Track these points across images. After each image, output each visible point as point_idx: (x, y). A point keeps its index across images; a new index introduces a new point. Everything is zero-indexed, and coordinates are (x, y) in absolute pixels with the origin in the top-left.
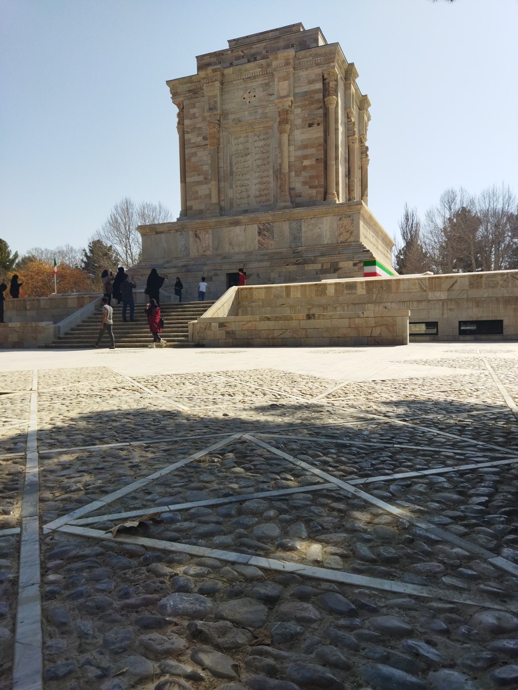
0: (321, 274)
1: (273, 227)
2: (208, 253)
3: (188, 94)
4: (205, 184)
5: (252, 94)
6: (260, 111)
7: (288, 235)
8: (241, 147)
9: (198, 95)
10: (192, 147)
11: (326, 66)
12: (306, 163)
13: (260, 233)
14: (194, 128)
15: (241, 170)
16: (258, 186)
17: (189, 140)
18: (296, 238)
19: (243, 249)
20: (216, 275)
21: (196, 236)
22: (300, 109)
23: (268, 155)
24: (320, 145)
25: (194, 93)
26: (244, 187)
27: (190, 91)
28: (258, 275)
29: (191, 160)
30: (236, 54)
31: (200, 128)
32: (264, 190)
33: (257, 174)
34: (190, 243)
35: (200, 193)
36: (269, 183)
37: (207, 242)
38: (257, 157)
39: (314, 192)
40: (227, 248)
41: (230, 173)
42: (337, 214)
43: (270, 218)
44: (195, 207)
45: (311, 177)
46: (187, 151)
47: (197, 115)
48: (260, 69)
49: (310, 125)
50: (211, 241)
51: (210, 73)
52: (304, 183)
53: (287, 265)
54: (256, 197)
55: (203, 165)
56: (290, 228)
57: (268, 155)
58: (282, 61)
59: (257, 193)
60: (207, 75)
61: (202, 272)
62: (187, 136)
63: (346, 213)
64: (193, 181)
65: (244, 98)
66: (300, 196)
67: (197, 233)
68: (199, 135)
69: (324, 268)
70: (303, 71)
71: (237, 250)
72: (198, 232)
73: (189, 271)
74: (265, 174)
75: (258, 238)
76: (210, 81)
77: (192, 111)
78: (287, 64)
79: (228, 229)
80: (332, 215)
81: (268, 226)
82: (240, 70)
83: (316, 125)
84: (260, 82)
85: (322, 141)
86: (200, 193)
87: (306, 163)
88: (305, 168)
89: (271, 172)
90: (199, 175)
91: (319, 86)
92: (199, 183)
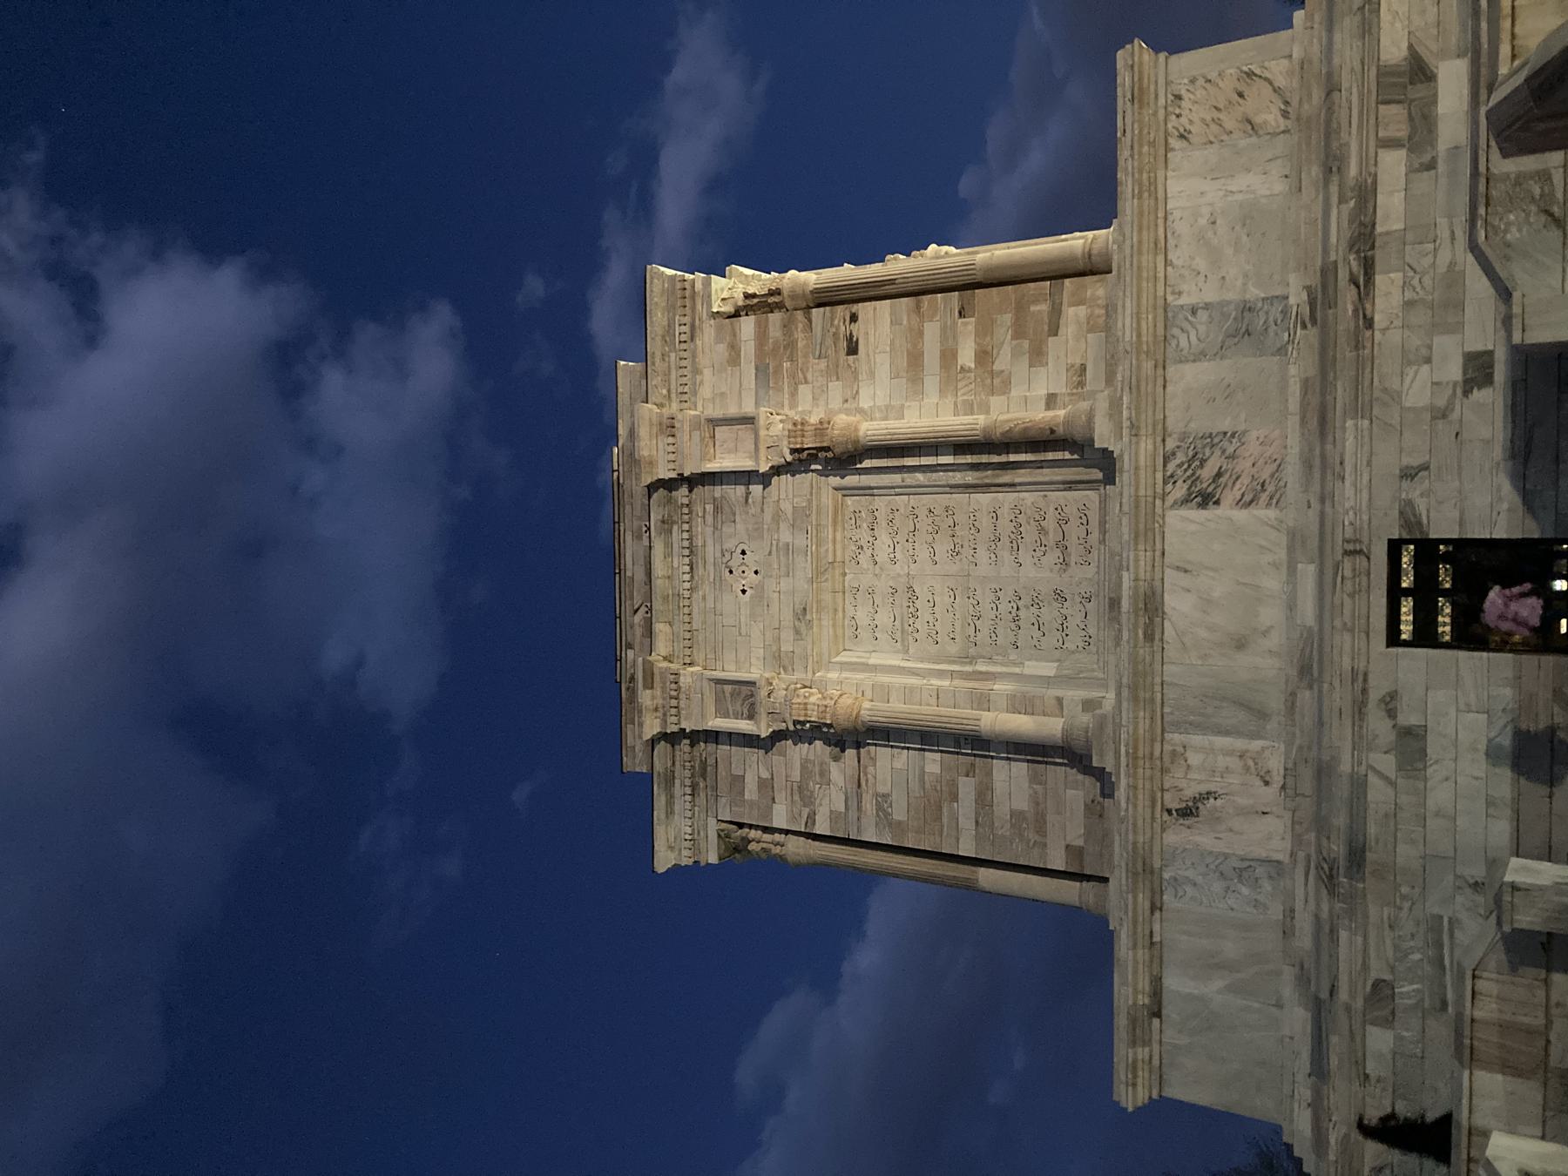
0: (1432, 143)
1: (1183, 437)
2: (1275, 764)
3: (702, 795)
4: (989, 774)
6: (785, 536)
7: (1227, 362)
8: (884, 618)
9: (711, 761)
10: (859, 808)
11: (699, 307)
12: (966, 356)
13: (1206, 500)
14: (803, 794)
15: (958, 624)
16: (1025, 556)
17: (834, 817)
18: (1243, 327)
19: (1273, 583)
20: (1390, 704)
21: (1187, 812)
22: (801, 387)
23: (922, 513)
24: (918, 307)
25: (704, 775)
26: (1022, 613)
27: (694, 787)
28: (1409, 474)
29: (900, 823)
30: (638, 631)
32: (1042, 531)
33: (983, 555)
34: (1220, 847)
35: (1022, 803)
36: (1018, 510)
37: (1222, 761)
38: (923, 553)
39: (1074, 315)
40: (1266, 665)
41: (963, 663)
42: (1162, 151)
43: (1146, 445)
44: (1076, 836)
45: (1018, 334)
47: (765, 775)
48: (675, 527)
49: (853, 349)
50: (1221, 741)
51: (653, 698)
52: (1037, 355)
53: (1369, 323)
54: (1065, 563)
55: (923, 772)
56: (1200, 356)
57: (922, 513)
58: (661, 446)
59: (1054, 556)
60: (656, 710)
61: (1373, 779)
62: (822, 828)
63: (1161, 112)
65: (744, 592)
66: (1083, 368)
67: (1174, 805)
68: (824, 773)
69: (1401, 130)
70: (702, 382)
71: (1270, 615)
73: (1357, 856)
74: (985, 522)
75: (1226, 511)
76: (674, 702)
77: (751, 792)
79: (1171, 652)
80: (1160, 174)
81: (1180, 457)
82: (666, 598)
84: (709, 530)
85: (904, 301)
86: (1022, 803)
89: (984, 499)
91: (747, 325)
92: (984, 797)
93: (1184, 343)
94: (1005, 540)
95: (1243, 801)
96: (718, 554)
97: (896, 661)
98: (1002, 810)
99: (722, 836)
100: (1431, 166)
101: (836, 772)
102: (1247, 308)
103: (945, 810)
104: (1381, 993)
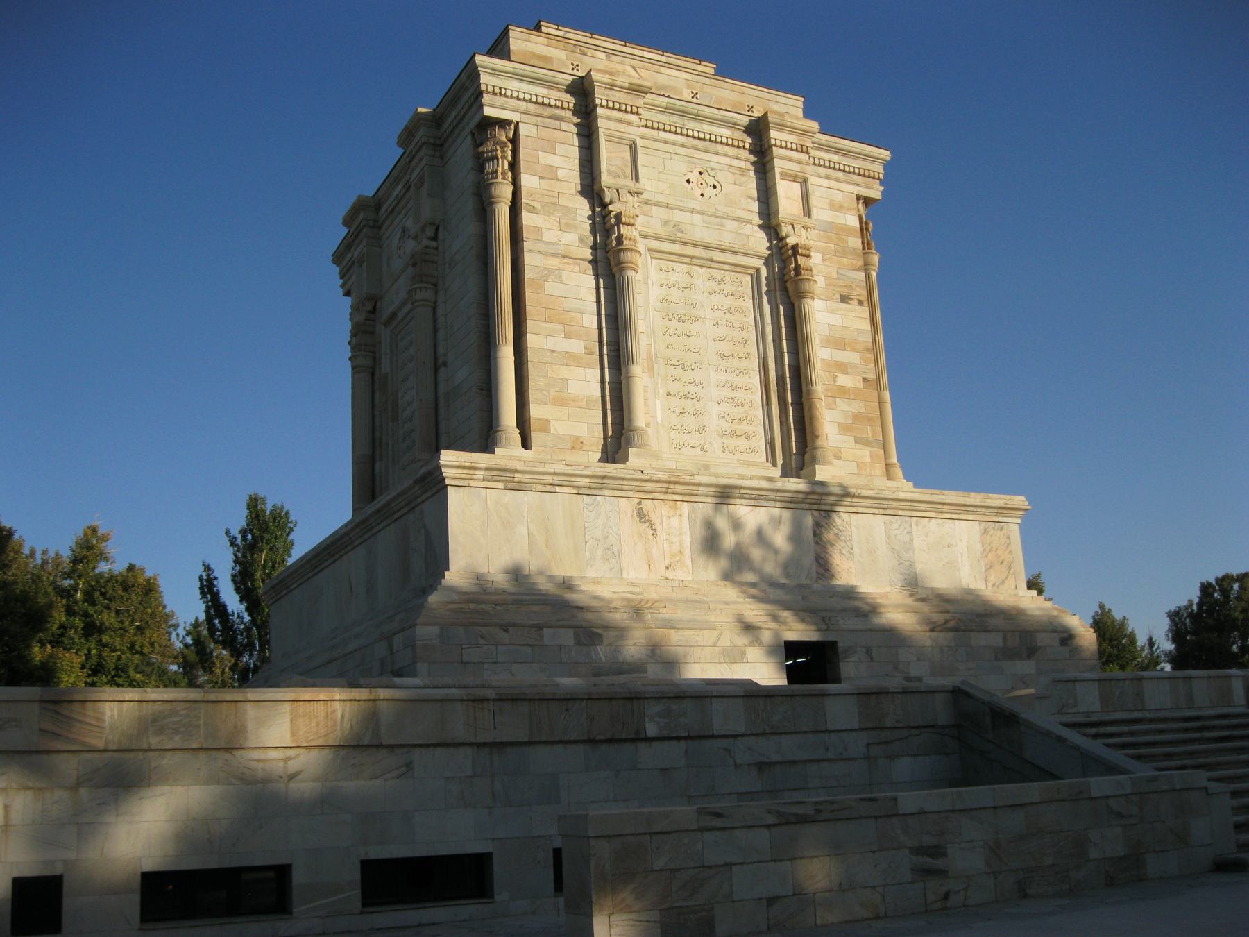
5: (711, 181)
10: (547, 254)
12: (843, 380)
14: (552, 206)
16: (725, 408)
21: (640, 513)
24: (868, 350)
25: (554, 117)
28: (868, 651)
29: (542, 287)
31: (567, 210)
32: (741, 421)
38: (722, 331)
39: (865, 453)
45: (856, 417)
47: (561, 174)
49: (844, 299)
52: (844, 428)
59: (727, 428)
61: (716, 633)
64: (550, 347)
72: (647, 505)
77: (546, 159)
78: (802, 150)
83: (855, 302)
86: (573, 388)
89: (755, 380)
90: (568, 336)
92: (569, 359)
93: (895, 526)
94: (733, 394)
95: (654, 550)
96: (713, 165)
98: (565, 372)
99: (503, 123)
100: (997, 659)
101: (570, 238)
103: (557, 326)
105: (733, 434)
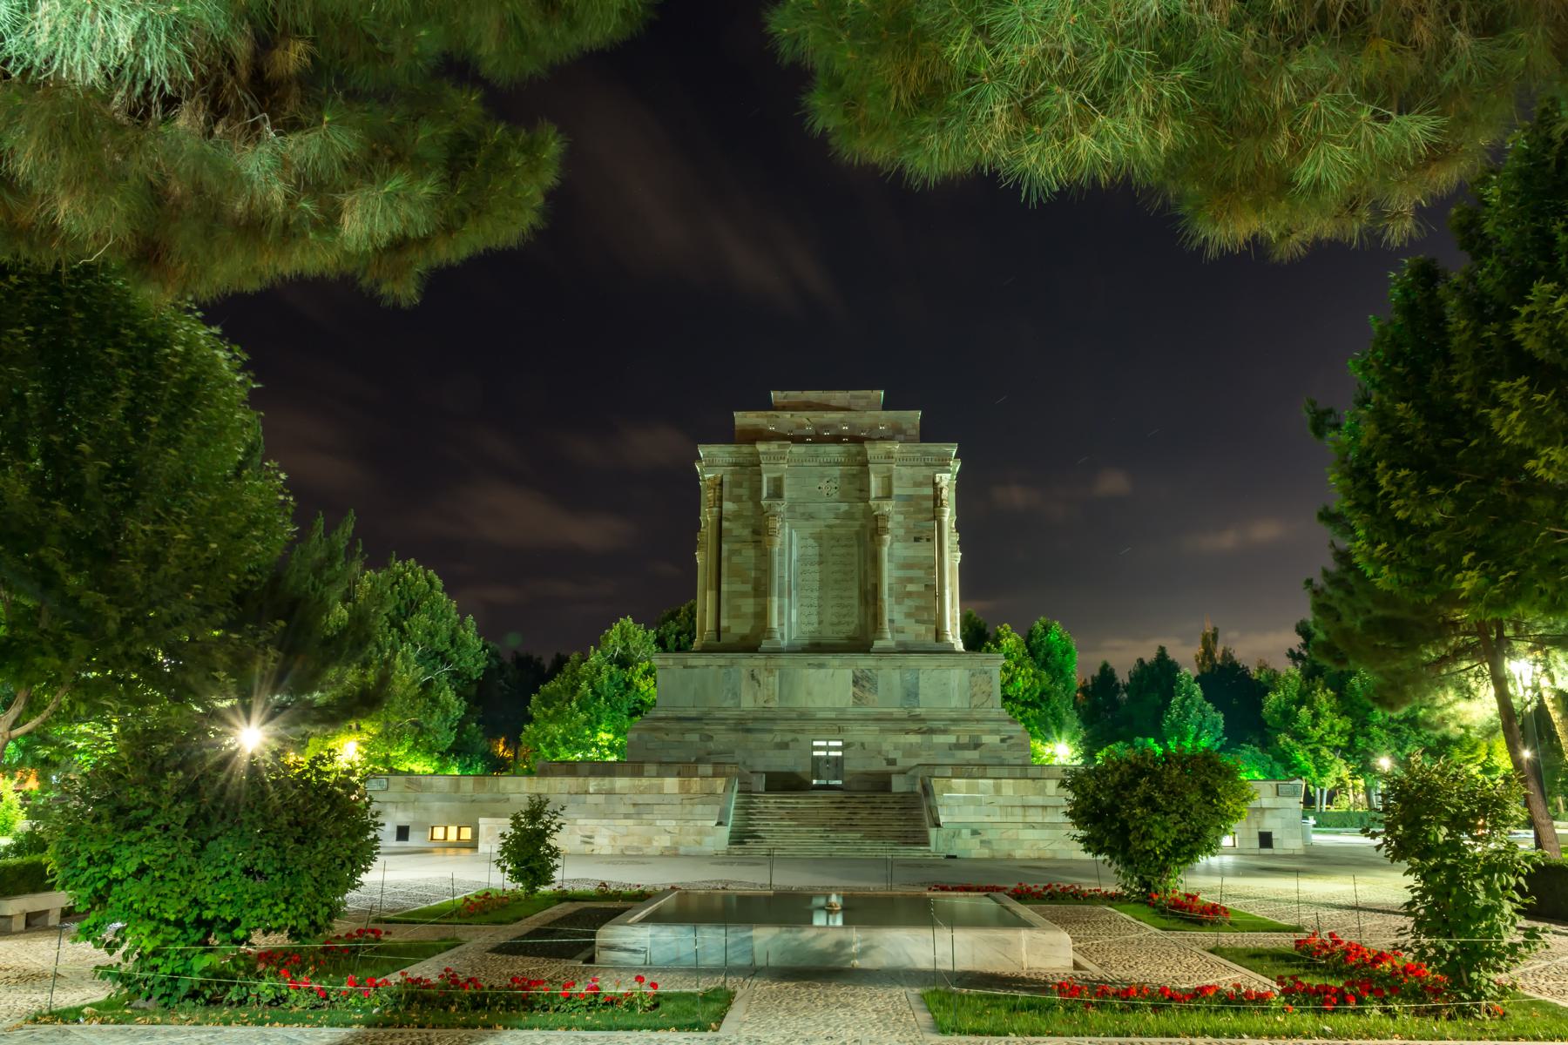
12: (910, 588)
13: (855, 683)
17: (730, 530)
21: (753, 676)
39: (922, 629)
45: (917, 608)
46: (725, 547)
49: (917, 540)
52: (908, 615)
54: (832, 624)
59: (835, 620)
62: (725, 524)
75: (852, 689)
87: (910, 588)
88: (910, 594)
89: (856, 593)
97: (794, 557)
102: (917, 695)
104: (710, 738)
105: (839, 623)
